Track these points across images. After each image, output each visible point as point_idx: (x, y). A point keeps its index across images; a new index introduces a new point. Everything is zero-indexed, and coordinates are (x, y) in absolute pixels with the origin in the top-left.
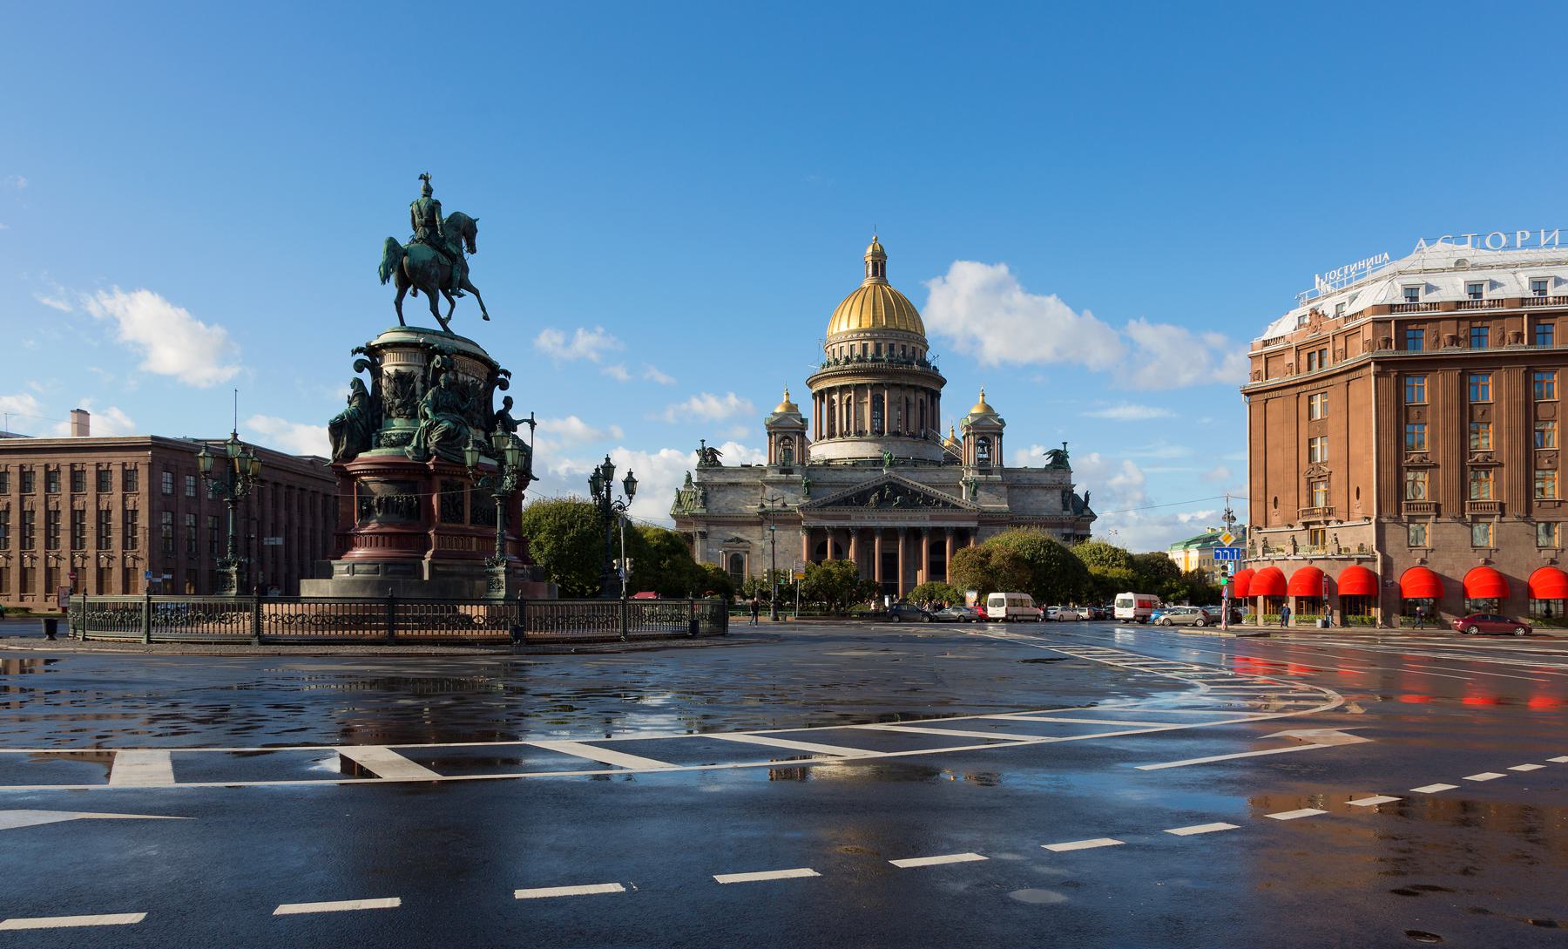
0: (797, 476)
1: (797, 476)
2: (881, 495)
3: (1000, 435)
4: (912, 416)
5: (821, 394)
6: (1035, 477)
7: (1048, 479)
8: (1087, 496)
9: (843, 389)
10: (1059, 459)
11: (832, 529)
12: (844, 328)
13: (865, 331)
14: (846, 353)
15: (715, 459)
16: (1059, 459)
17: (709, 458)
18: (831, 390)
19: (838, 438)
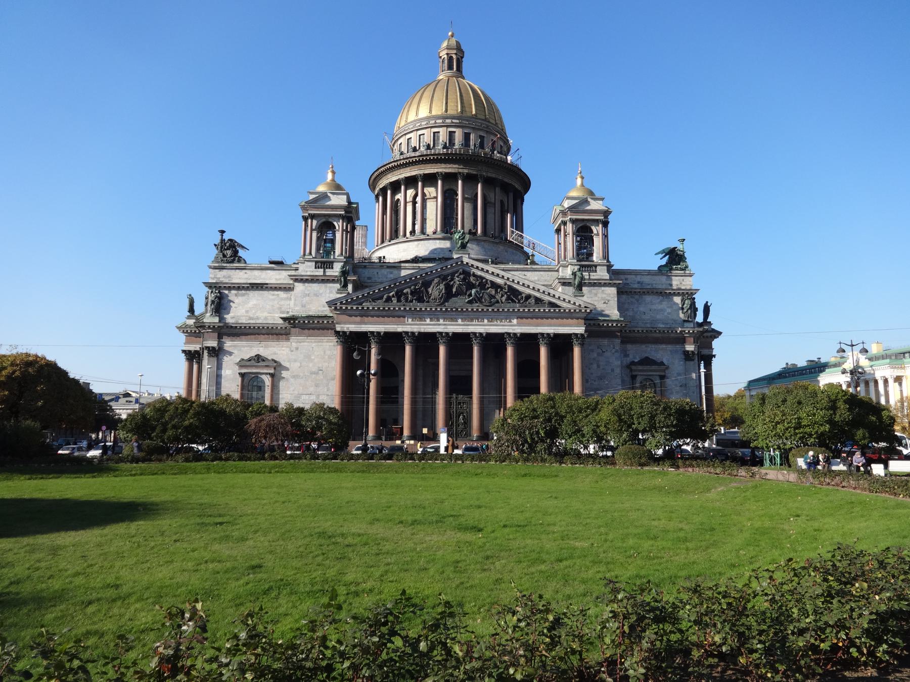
2: (448, 288)
3: (605, 224)
4: (490, 216)
5: (384, 191)
6: (646, 279)
8: (707, 309)
9: (411, 182)
10: (675, 258)
11: (379, 333)
12: (412, 117)
13: (437, 117)
14: (414, 143)
15: (236, 252)
16: (675, 258)
17: (230, 252)
18: (395, 187)
19: (401, 239)
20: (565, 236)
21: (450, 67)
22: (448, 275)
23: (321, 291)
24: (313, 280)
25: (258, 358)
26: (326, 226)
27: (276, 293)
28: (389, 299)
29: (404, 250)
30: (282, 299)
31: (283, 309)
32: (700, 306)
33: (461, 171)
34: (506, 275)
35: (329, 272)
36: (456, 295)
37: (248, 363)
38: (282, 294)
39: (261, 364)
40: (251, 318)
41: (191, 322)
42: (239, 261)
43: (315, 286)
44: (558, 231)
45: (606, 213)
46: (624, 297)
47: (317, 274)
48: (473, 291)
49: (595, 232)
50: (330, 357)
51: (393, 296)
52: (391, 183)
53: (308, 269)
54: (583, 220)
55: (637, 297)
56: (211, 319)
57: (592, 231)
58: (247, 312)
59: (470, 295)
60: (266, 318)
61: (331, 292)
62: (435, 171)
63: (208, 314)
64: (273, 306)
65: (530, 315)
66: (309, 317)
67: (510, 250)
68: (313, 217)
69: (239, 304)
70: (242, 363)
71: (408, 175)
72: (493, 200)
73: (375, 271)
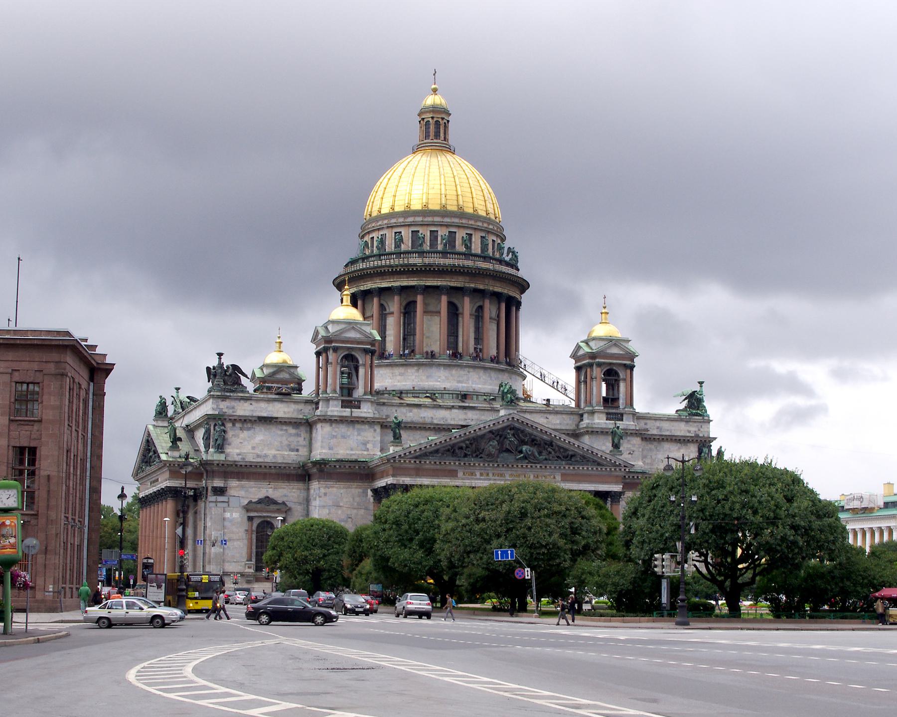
0: (366, 410)
1: (366, 410)
3: (632, 368)
7: (681, 429)
16: (695, 402)
20: (592, 378)
21: (437, 135)
22: (498, 430)
23: (349, 433)
24: (342, 420)
25: (267, 501)
26: (350, 361)
27: (285, 428)
28: (443, 454)
29: (401, 374)
30: (291, 435)
31: (292, 447)
32: (714, 453)
33: (467, 285)
34: (554, 433)
35: (356, 413)
36: (508, 451)
37: (259, 506)
38: (292, 431)
39: (273, 507)
40: (258, 456)
41: (176, 454)
42: (242, 392)
43: (343, 429)
44: (578, 369)
45: (632, 356)
46: (644, 443)
47: (344, 414)
48: (524, 448)
49: (622, 375)
50: (358, 504)
51: (449, 450)
52: (380, 288)
53: (335, 409)
54: (610, 364)
55: (655, 443)
56: (212, 455)
57: (617, 374)
58: (253, 448)
59: (521, 452)
60: (275, 456)
61: (359, 435)
62: (439, 284)
63: (211, 450)
64: (281, 442)
65: (574, 472)
66: (337, 461)
67: (514, 376)
68: (336, 350)
69: (245, 440)
70: (248, 508)
71: (405, 284)
72: (494, 314)
73: (394, 409)
